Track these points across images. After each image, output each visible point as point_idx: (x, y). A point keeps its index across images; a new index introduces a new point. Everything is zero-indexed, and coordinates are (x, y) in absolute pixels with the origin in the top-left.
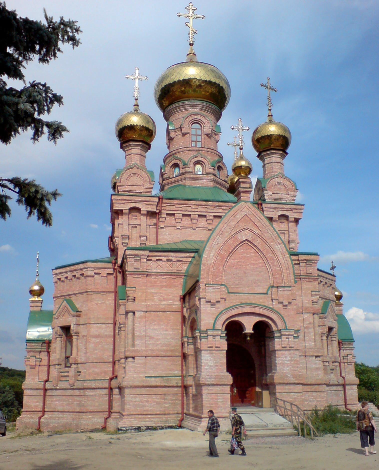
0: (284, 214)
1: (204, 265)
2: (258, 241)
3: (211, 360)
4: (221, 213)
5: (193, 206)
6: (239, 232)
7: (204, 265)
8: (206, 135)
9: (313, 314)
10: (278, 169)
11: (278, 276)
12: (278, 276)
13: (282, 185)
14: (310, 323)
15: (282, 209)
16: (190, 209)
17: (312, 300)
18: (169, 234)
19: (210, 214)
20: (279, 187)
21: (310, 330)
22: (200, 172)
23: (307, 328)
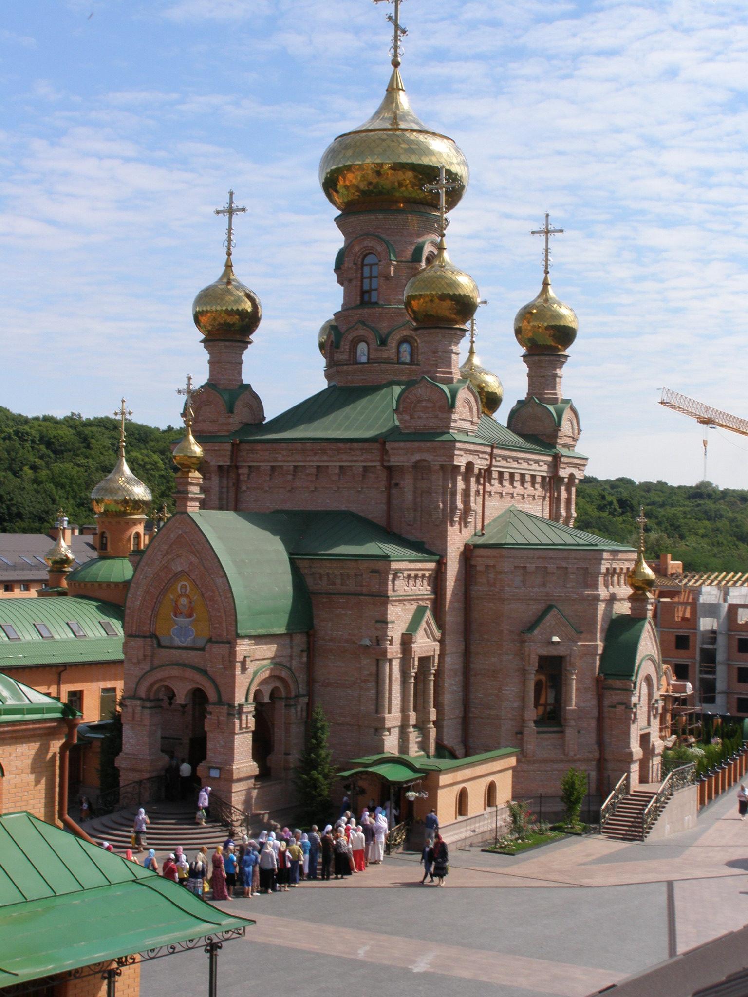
0: (423, 458)
1: (129, 609)
2: (196, 573)
3: (132, 737)
4: (326, 461)
5: (284, 453)
6: (173, 560)
7: (129, 609)
8: (383, 277)
9: (378, 660)
10: (434, 364)
11: (217, 625)
12: (217, 625)
13: (429, 400)
14: (370, 675)
15: (420, 450)
16: (280, 457)
17: (377, 637)
18: (254, 501)
19: (311, 464)
20: (424, 404)
21: (369, 685)
22: (364, 355)
23: (365, 681)
